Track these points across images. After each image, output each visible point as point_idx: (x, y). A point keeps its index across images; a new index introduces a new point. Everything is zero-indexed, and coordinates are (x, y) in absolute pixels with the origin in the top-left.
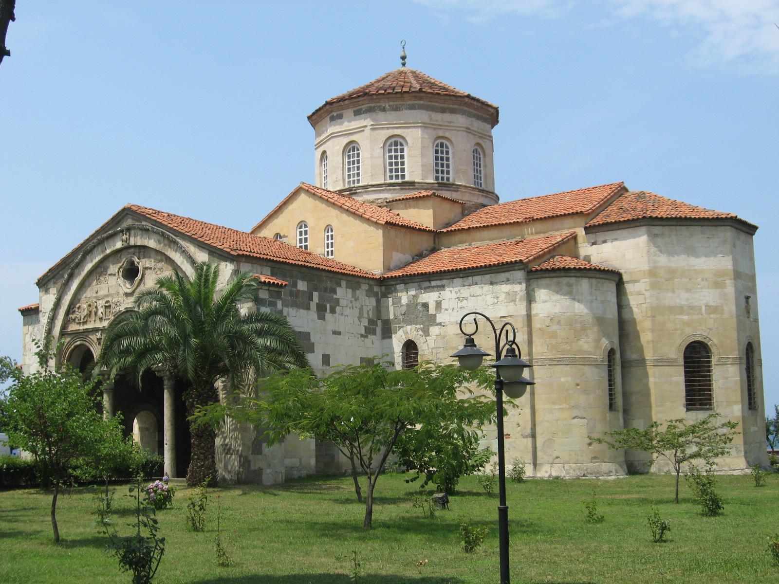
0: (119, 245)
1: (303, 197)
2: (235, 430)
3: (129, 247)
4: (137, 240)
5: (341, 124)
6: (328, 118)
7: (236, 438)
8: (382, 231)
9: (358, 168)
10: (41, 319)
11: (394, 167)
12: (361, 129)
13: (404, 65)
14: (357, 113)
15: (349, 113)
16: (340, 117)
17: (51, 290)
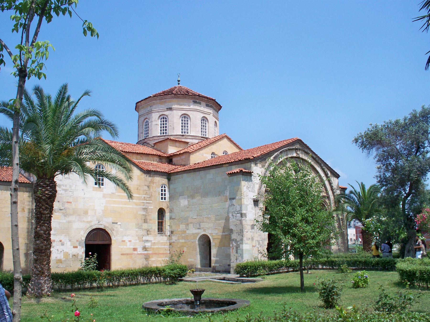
0: (295, 155)
1: (225, 140)
2: (341, 243)
3: (299, 158)
4: (302, 156)
5: (201, 107)
6: (192, 100)
7: (342, 246)
8: (371, 181)
9: (206, 129)
10: (253, 179)
11: (162, 126)
12: (209, 114)
13: (179, 84)
14: (207, 106)
15: (203, 104)
16: (200, 103)
17: (258, 165)
